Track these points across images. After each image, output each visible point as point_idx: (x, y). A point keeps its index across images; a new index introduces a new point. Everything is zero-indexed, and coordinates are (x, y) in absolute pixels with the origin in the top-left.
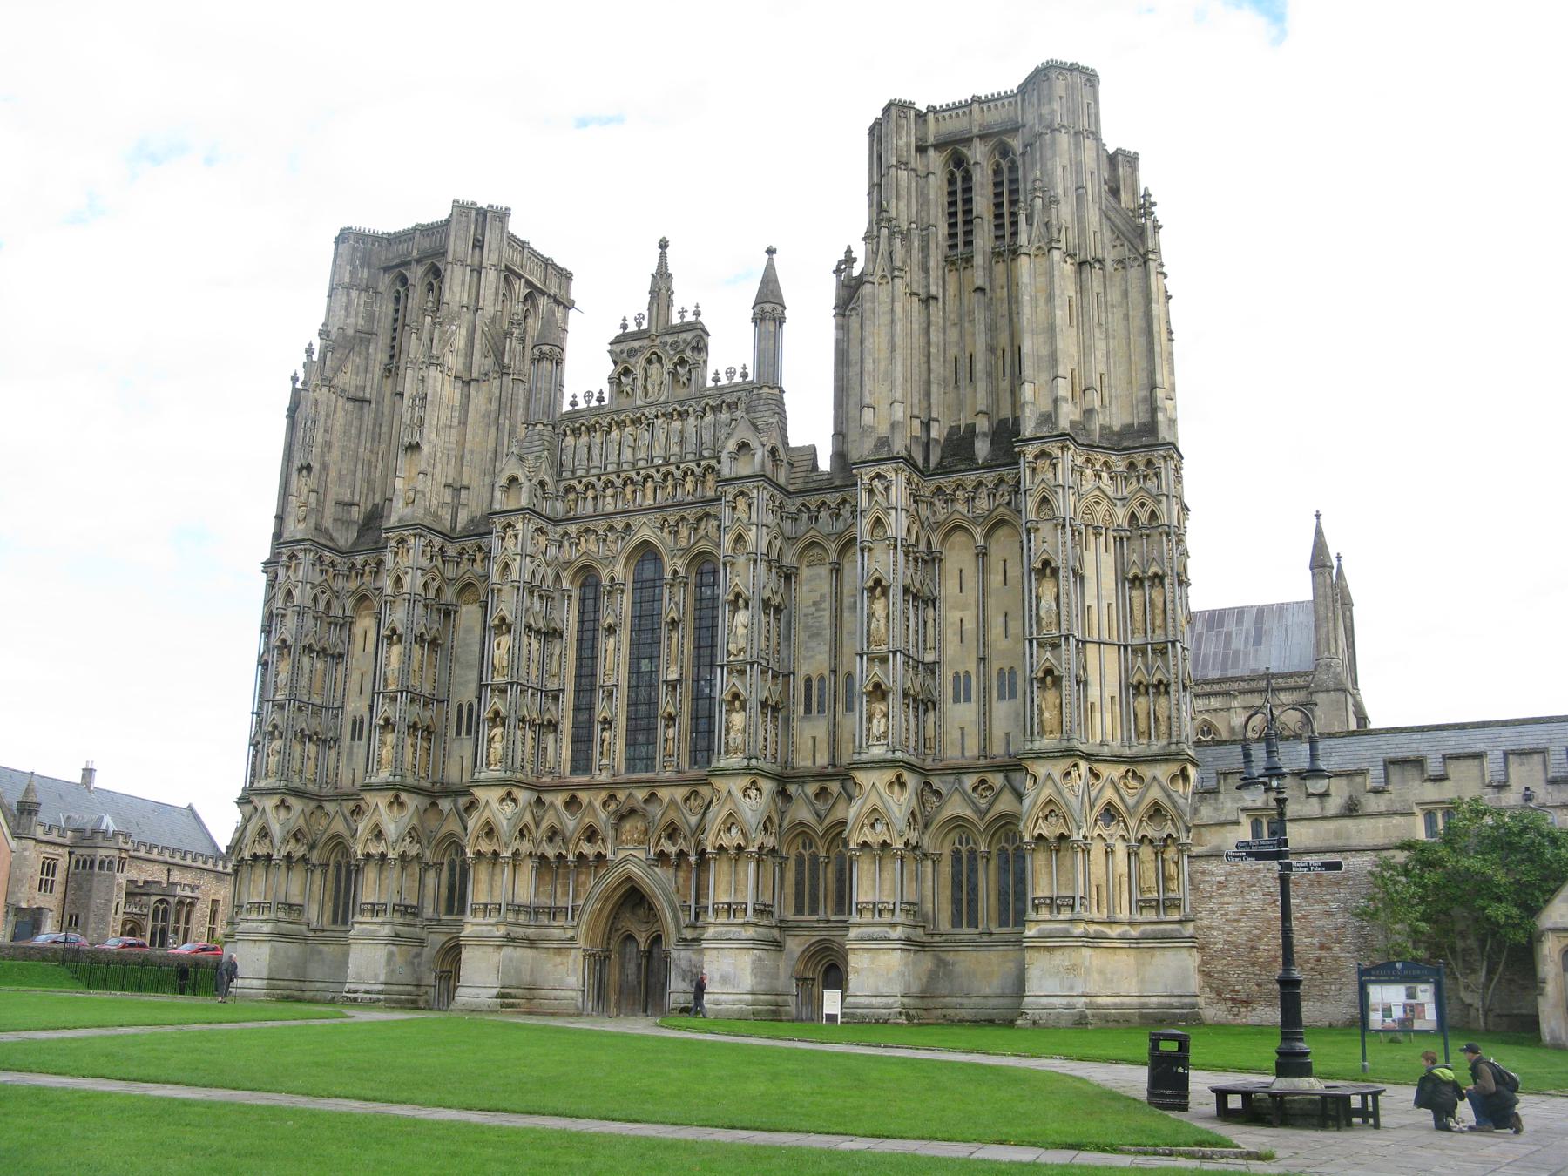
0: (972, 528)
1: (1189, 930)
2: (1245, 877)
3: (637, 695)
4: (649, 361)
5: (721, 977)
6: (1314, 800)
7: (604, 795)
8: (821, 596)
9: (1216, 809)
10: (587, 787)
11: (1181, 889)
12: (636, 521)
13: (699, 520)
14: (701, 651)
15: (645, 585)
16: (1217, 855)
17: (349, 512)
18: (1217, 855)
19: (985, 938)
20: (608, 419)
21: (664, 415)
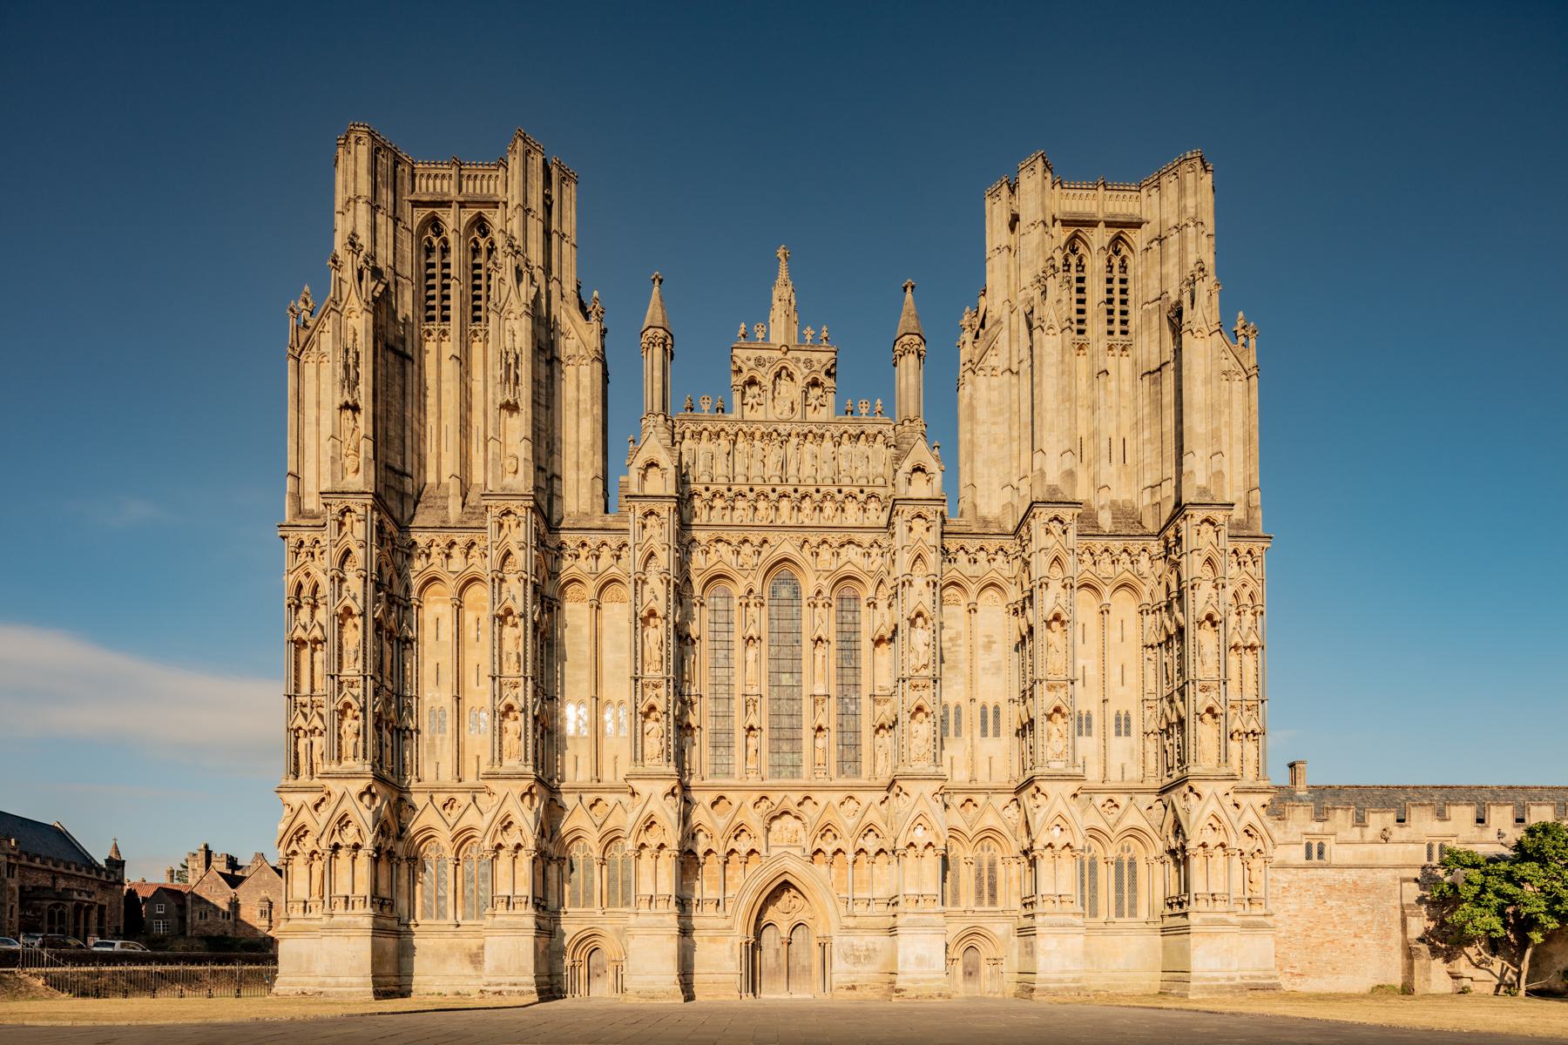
0: (1101, 587)
1: (1269, 920)
2: (1302, 884)
3: (779, 707)
4: (778, 375)
5: (917, 958)
6: (1357, 830)
7: (756, 796)
8: (957, 633)
9: (1285, 833)
10: (736, 789)
11: (1259, 890)
12: (773, 537)
13: (842, 546)
14: (845, 671)
15: (781, 602)
16: (1283, 866)
17: (402, 483)
18: (1283, 866)
19: (1111, 925)
20: (736, 429)
21: (798, 435)
